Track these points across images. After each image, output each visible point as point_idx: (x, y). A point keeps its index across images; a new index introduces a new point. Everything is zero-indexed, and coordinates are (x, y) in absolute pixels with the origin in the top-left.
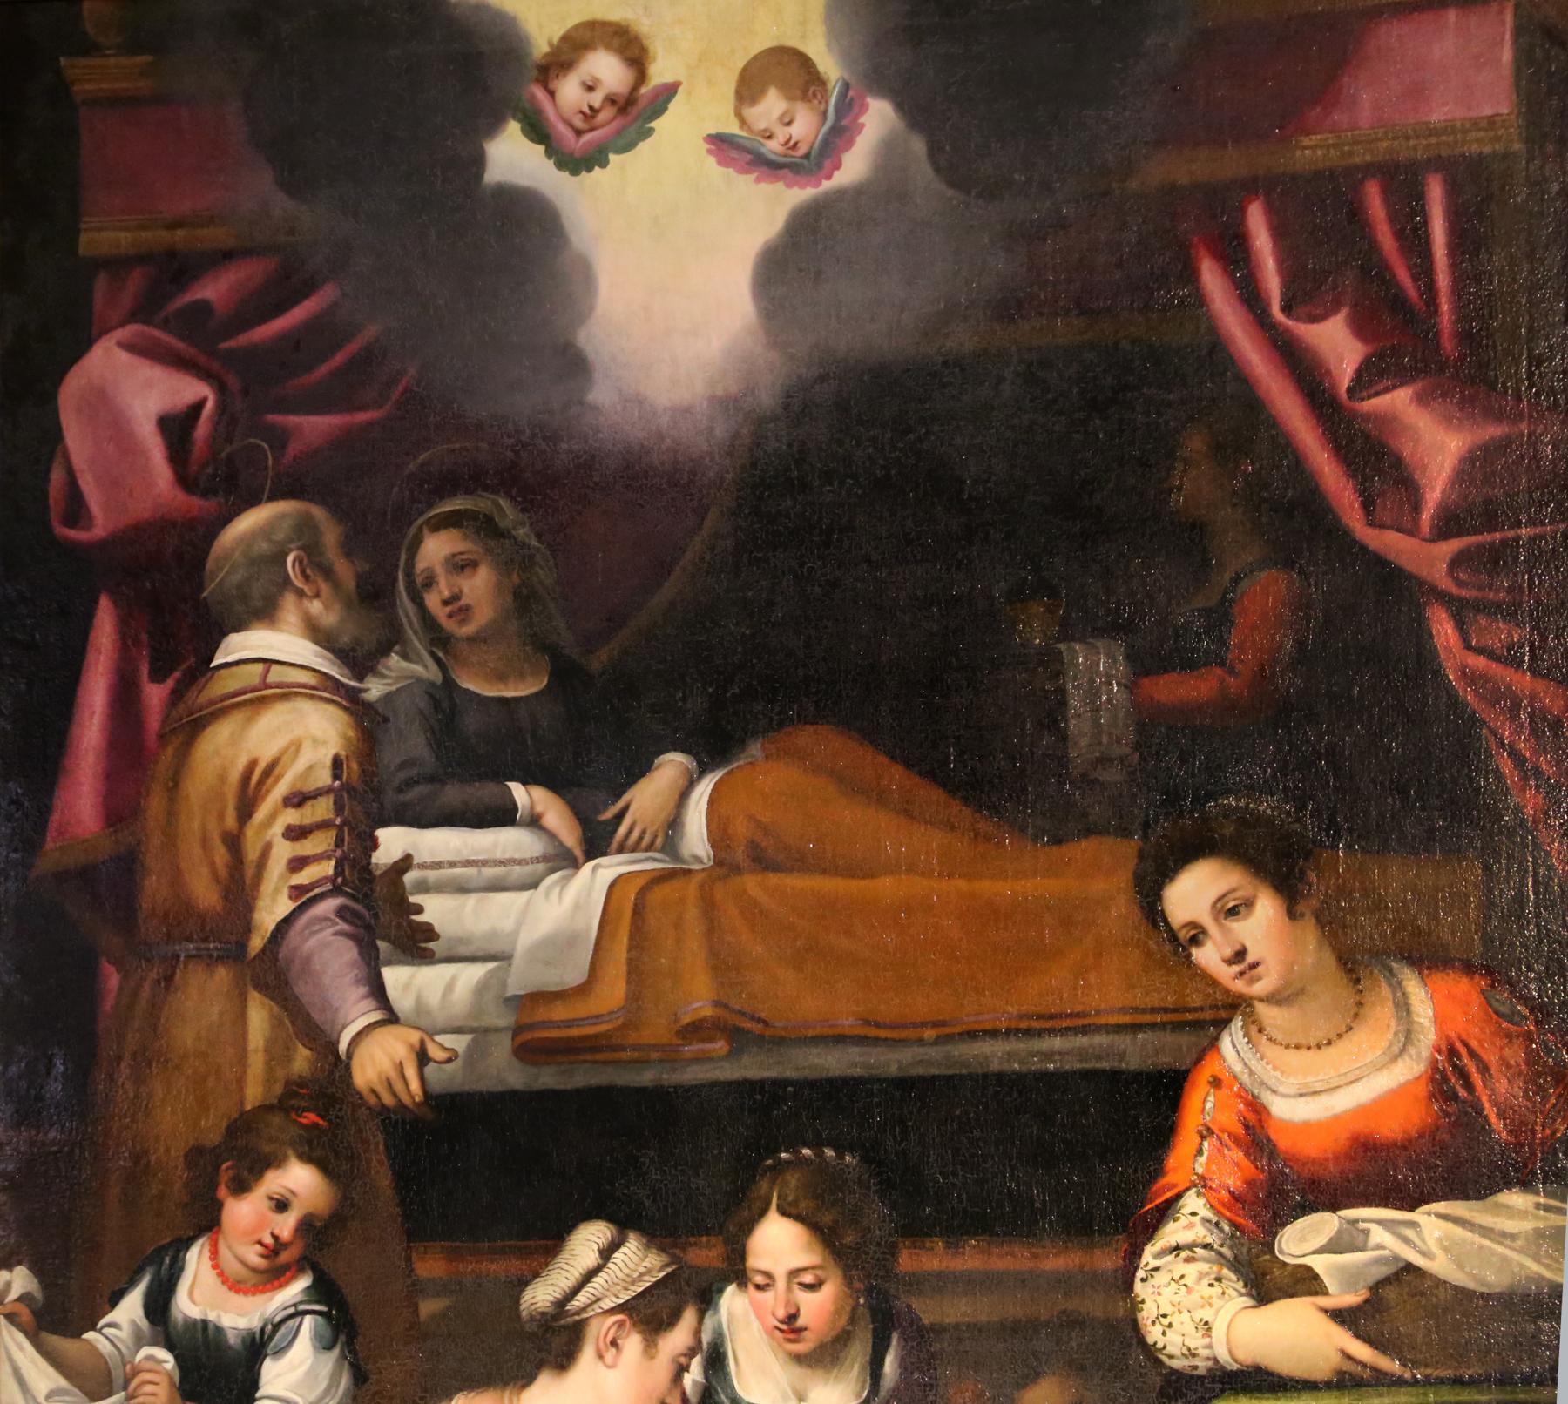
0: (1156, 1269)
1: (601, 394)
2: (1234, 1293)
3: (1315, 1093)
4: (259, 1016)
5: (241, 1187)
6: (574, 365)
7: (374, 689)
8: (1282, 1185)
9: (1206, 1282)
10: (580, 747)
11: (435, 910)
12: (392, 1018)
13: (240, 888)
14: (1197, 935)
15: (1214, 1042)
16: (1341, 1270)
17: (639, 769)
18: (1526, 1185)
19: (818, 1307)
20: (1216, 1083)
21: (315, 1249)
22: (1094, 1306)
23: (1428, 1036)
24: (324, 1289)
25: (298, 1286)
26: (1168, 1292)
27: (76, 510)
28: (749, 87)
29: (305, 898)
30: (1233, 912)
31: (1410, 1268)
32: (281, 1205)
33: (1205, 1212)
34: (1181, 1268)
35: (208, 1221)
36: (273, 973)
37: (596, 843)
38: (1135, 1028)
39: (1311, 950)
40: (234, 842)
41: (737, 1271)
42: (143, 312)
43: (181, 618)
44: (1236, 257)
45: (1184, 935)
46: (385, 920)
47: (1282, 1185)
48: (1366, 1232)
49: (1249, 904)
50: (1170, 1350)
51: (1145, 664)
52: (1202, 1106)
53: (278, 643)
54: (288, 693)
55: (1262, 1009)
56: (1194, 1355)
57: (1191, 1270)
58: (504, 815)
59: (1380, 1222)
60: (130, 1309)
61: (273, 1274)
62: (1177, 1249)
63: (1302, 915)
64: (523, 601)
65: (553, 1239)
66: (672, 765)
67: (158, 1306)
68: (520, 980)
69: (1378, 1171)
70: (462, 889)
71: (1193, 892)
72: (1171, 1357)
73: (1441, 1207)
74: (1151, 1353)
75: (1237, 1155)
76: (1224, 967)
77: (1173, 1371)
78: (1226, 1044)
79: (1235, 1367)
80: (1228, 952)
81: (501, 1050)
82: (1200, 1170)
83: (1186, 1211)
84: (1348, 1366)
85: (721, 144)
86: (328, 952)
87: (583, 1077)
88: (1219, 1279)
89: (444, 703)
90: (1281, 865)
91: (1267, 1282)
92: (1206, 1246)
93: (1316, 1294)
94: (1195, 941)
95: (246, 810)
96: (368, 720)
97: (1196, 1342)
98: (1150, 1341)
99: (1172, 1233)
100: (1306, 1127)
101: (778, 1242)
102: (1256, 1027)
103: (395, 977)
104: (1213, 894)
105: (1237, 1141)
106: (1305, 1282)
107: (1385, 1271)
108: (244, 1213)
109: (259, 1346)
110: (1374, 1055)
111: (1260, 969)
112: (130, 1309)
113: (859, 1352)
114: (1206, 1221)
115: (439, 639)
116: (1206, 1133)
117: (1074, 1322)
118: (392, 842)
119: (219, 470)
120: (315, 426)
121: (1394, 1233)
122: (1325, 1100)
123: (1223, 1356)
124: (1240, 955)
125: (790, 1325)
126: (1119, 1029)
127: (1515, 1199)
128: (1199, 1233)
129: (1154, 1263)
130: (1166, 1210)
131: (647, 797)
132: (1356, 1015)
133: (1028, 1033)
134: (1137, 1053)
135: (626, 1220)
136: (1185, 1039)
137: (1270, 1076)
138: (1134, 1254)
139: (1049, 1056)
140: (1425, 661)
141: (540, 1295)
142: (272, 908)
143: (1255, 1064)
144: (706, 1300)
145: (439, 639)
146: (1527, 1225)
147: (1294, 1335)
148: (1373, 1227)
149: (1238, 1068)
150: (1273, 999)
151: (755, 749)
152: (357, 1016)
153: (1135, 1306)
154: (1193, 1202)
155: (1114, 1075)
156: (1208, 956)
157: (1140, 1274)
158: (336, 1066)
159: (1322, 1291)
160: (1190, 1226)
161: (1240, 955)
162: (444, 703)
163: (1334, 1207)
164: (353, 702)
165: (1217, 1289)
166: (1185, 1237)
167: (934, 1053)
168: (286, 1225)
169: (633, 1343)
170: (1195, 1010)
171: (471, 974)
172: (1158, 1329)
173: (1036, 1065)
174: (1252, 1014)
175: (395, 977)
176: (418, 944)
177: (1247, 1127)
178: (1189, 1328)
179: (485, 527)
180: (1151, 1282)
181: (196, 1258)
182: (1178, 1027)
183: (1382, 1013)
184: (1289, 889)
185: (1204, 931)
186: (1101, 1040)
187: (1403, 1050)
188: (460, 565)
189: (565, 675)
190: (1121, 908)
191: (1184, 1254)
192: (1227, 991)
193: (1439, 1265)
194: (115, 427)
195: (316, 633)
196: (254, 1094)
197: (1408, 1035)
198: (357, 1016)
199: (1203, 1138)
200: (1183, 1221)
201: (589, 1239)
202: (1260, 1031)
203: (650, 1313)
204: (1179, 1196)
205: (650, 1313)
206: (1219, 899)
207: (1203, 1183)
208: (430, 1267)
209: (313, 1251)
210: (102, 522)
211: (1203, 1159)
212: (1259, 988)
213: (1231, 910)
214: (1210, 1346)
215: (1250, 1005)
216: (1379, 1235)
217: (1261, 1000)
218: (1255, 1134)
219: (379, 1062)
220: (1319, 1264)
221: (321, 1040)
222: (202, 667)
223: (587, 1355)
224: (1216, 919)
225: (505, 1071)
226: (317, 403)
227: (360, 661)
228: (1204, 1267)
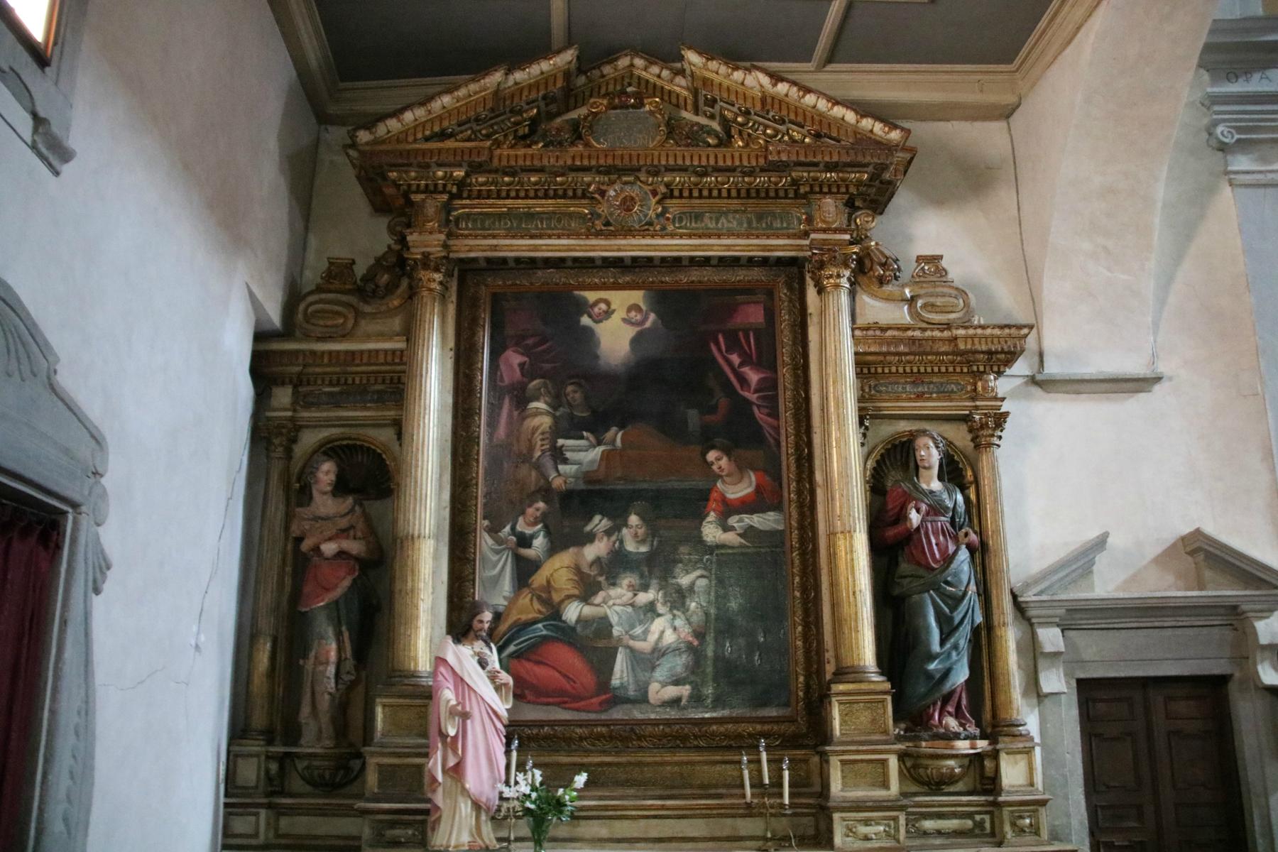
1: (601, 362)
4: (534, 473)
5: (530, 506)
6: (597, 357)
7: (558, 414)
10: (595, 424)
11: (568, 455)
12: (560, 475)
13: (531, 449)
14: (712, 463)
17: (607, 430)
18: (774, 510)
19: (641, 532)
21: (543, 519)
23: (754, 484)
24: (546, 527)
25: (540, 526)
27: (502, 380)
28: (629, 310)
29: (543, 452)
32: (538, 510)
35: (523, 513)
36: (538, 466)
37: (599, 443)
40: (530, 441)
41: (626, 525)
42: (517, 344)
43: (521, 400)
44: (717, 344)
46: (559, 456)
47: (729, 509)
52: (714, 495)
53: (540, 405)
54: (541, 414)
58: (582, 438)
60: (508, 528)
61: (535, 524)
64: (586, 398)
65: (590, 519)
66: (614, 429)
67: (513, 528)
68: (584, 469)
70: (573, 451)
71: (712, 456)
81: (581, 482)
85: (624, 320)
86: (548, 462)
87: (598, 487)
89: (571, 417)
90: (727, 451)
95: (533, 434)
96: (556, 420)
101: (634, 519)
102: (724, 482)
103: (560, 467)
108: (530, 511)
109: (533, 537)
112: (508, 528)
113: (649, 539)
115: (570, 405)
118: (561, 442)
119: (529, 372)
120: (547, 366)
125: (636, 535)
130: (707, 515)
131: (609, 435)
134: (701, 484)
135: (604, 515)
140: (753, 414)
141: (588, 528)
142: (537, 454)
144: (619, 530)
145: (570, 405)
150: (727, 475)
151: (630, 427)
152: (553, 474)
154: (712, 513)
156: (715, 467)
158: (549, 483)
162: (571, 417)
164: (554, 417)
168: (538, 514)
169: (605, 539)
171: (575, 467)
175: (560, 467)
176: (565, 461)
179: (579, 385)
181: (521, 519)
183: (746, 480)
188: (575, 392)
189: (594, 412)
194: (511, 366)
195: (546, 403)
196: (533, 488)
198: (553, 474)
201: (597, 518)
203: (608, 533)
205: (608, 533)
208: (566, 523)
209: (543, 519)
210: (507, 381)
213: (718, 459)
218: (724, 500)
219: (557, 483)
221: (546, 479)
222: (525, 409)
223: (596, 542)
225: (582, 486)
226: (548, 361)
227: (555, 408)
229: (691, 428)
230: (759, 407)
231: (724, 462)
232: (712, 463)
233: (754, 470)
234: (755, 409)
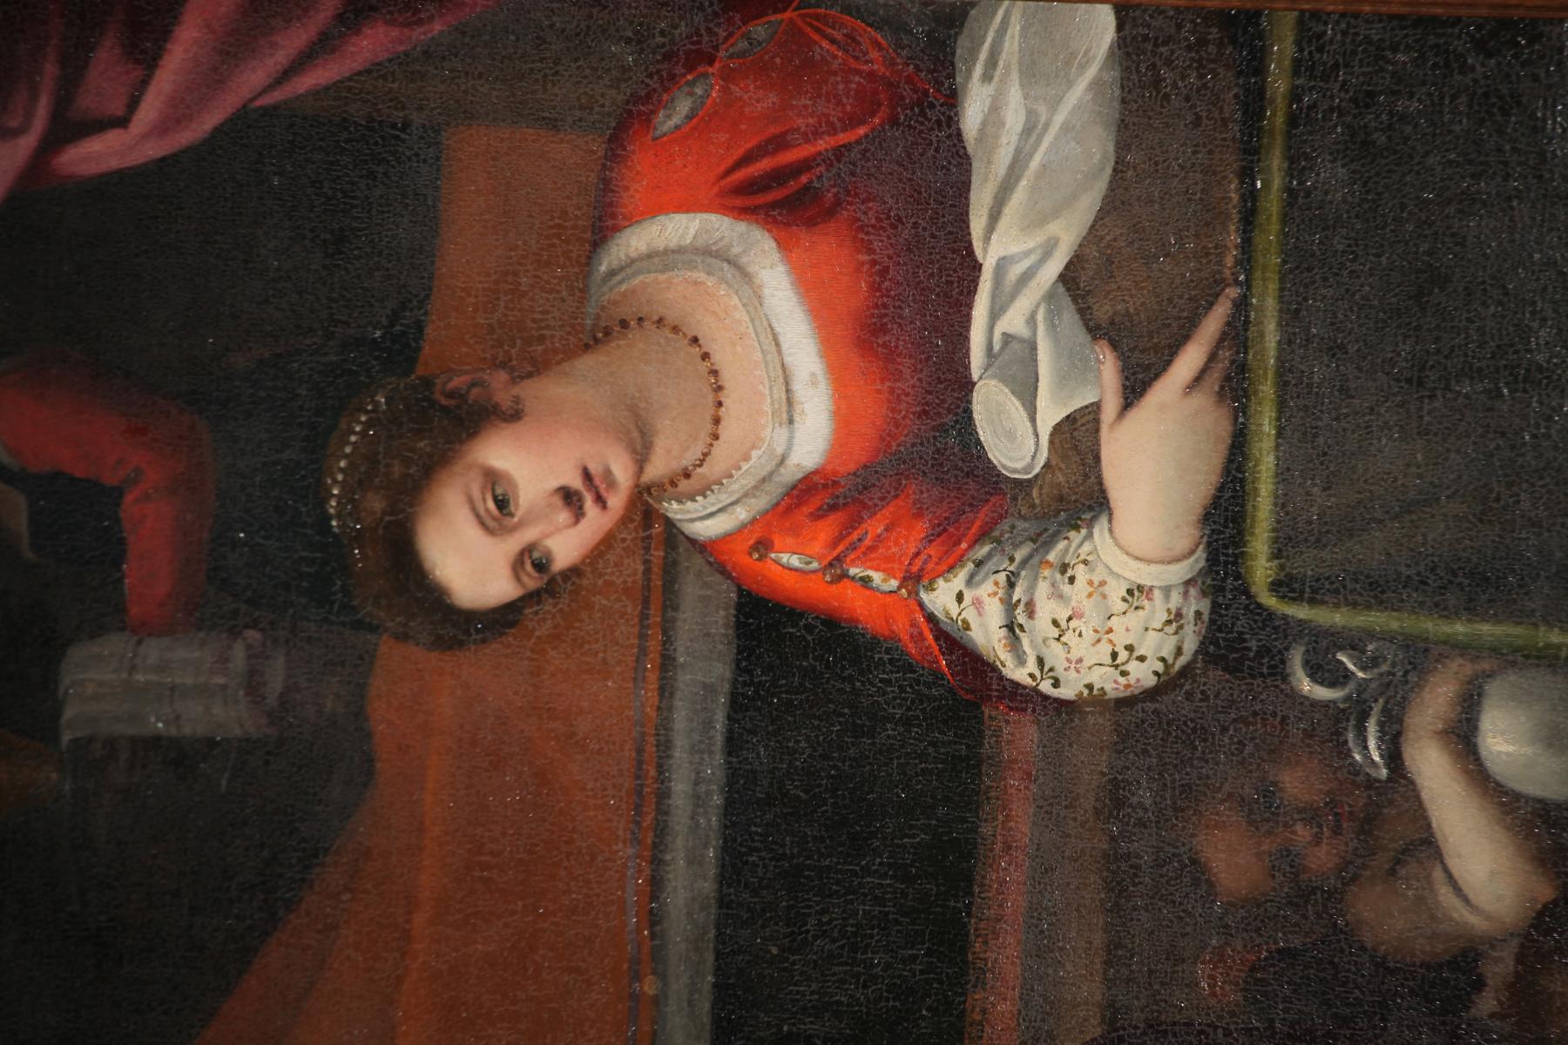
0: (1041, 662)
2: (1087, 547)
3: (790, 402)
8: (924, 463)
9: (1066, 588)
14: (532, 559)
15: (701, 547)
16: (1063, 380)
20: (763, 546)
22: (1090, 763)
26: (1079, 647)
30: (502, 504)
31: (1068, 278)
33: (958, 581)
34: (1042, 624)
38: (667, 662)
39: (575, 388)
45: (533, 581)
47: (924, 463)
48: (1008, 338)
49: (492, 478)
50: (1167, 652)
51: (108, 613)
55: (657, 469)
56: (1179, 615)
57: (1047, 608)
59: (995, 315)
62: (1011, 627)
63: (517, 400)
69: (910, 316)
71: (466, 560)
72: (1179, 651)
73: (977, 225)
74: (1169, 682)
75: (874, 527)
76: (584, 523)
77: (1202, 650)
78: (708, 529)
79: (1201, 554)
80: (564, 516)
82: (894, 583)
83: (954, 609)
84: (1213, 381)
88: (1064, 568)
91: (1073, 493)
92: (1011, 585)
93: (1097, 421)
94: (541, 566)
97: (1157, 611)
98: (1151, 681)
99: (987, 633)
100: (844, 420)
102: (681, 481)
104: (470, 531)
105: (854, 523)
106: (1078, 437)
107: (1070, 317)
110: (732, 301)
111: (595, 468)
114: (970, 582)
116: (835, 567)
117: (1115, 797)
121: (1013, 296)
122: (799, 387)
123: (1180, 572)
124: (569, 497)
126: (666, 690)
127: (972, 116)
128: (989, 592)
129: (1032, 666)
130: (952, 642)
132: (675, 329)
133: (661, 831)
134: (705, 661)
136: (691, 589)
137: (759, 461)
138: (1017, 696)
139: (698, 801)
143: (736, 487)
146: (1014, 95)
147: (1157, 460)
148: (1002, 326)
149: (742, 514)
150: (641, 458)
153: (1094, 700)
154: (942, 598)
155: (737, 705)
156: (567, 545)
157: (1046, 687)
159: (1094, 410)
160: (977, 603)
161: (569, 497)
163: (966, 385)
165: (1080, 572)
166: (994, 614)
167: (679, 983)
170: (647, 571)
172: (1133, 667)
173: (712, 820)
174: (660, 486)
177: (833, 508)
178: (1135, 620)
180: (1060, 672)
182: (670, 601)
183: (675, 292)
184: (471, 418)
185: (529, 549)
186: (681, 719)
187: (733, 262)
190: (483, 670)
191: (1021, 618)
192: (625, 520)
193: (1067, 233)
197: (710, 254)
199: (845, 575)
200: (970, 615)
202: (687, 475)
204: (931, 618)
206: (483, 524)
207: (915, 579)
211: (877, 577)
212: (623, 473)
213: (500, 506)
214: (1167, 590)
215: (648, 489)
216: (1014, 321)
217: (640, 470)
220: (1050, 413)
224: (512, 530)
228: (1043, 588)
229: (229, 717)
230: (69, 127)
231: (530, 462)
232: (532, 559)
233: (604, 224)
234: (96, 155)
